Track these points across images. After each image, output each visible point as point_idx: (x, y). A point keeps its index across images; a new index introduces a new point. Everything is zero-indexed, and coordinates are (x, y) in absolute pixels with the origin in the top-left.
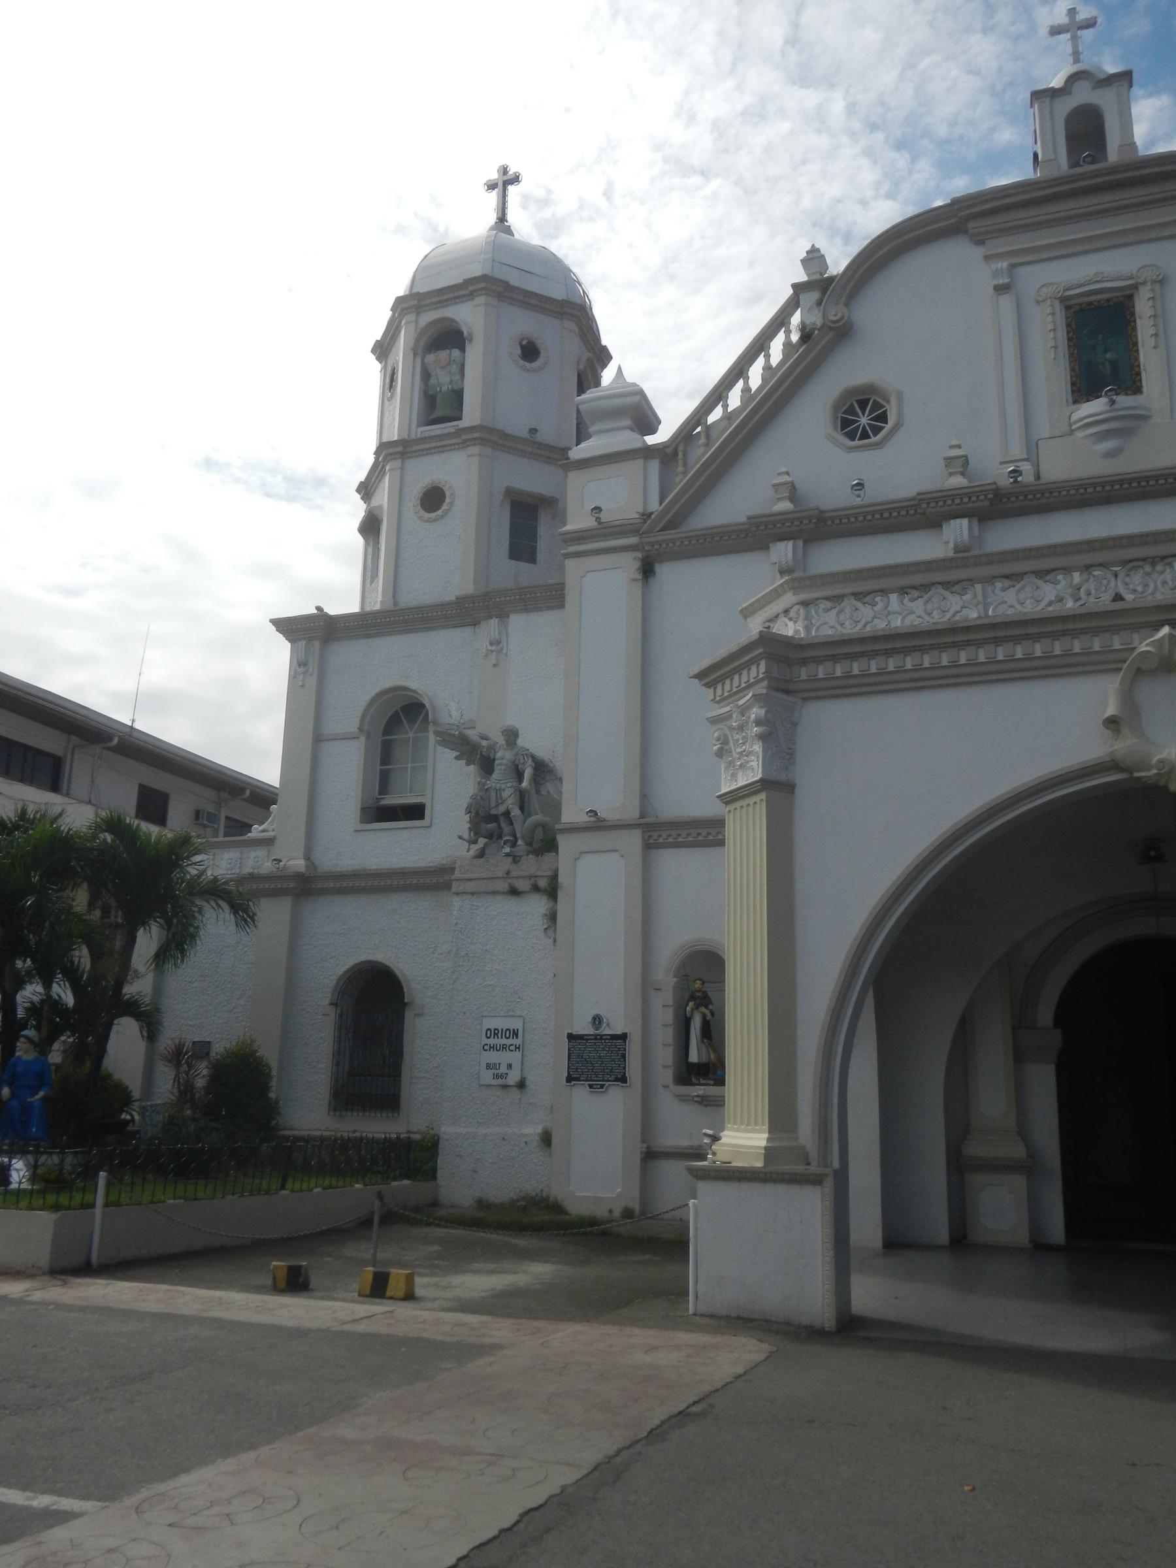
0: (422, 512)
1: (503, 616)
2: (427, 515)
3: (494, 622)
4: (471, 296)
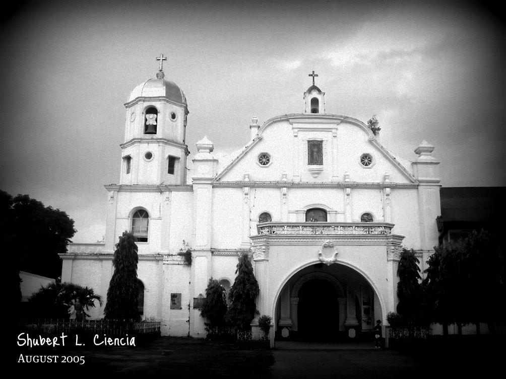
0: (145, 157)
1: (170, 191)
2: (146, 159)
3: (167, 193)
4: (160, 100)
